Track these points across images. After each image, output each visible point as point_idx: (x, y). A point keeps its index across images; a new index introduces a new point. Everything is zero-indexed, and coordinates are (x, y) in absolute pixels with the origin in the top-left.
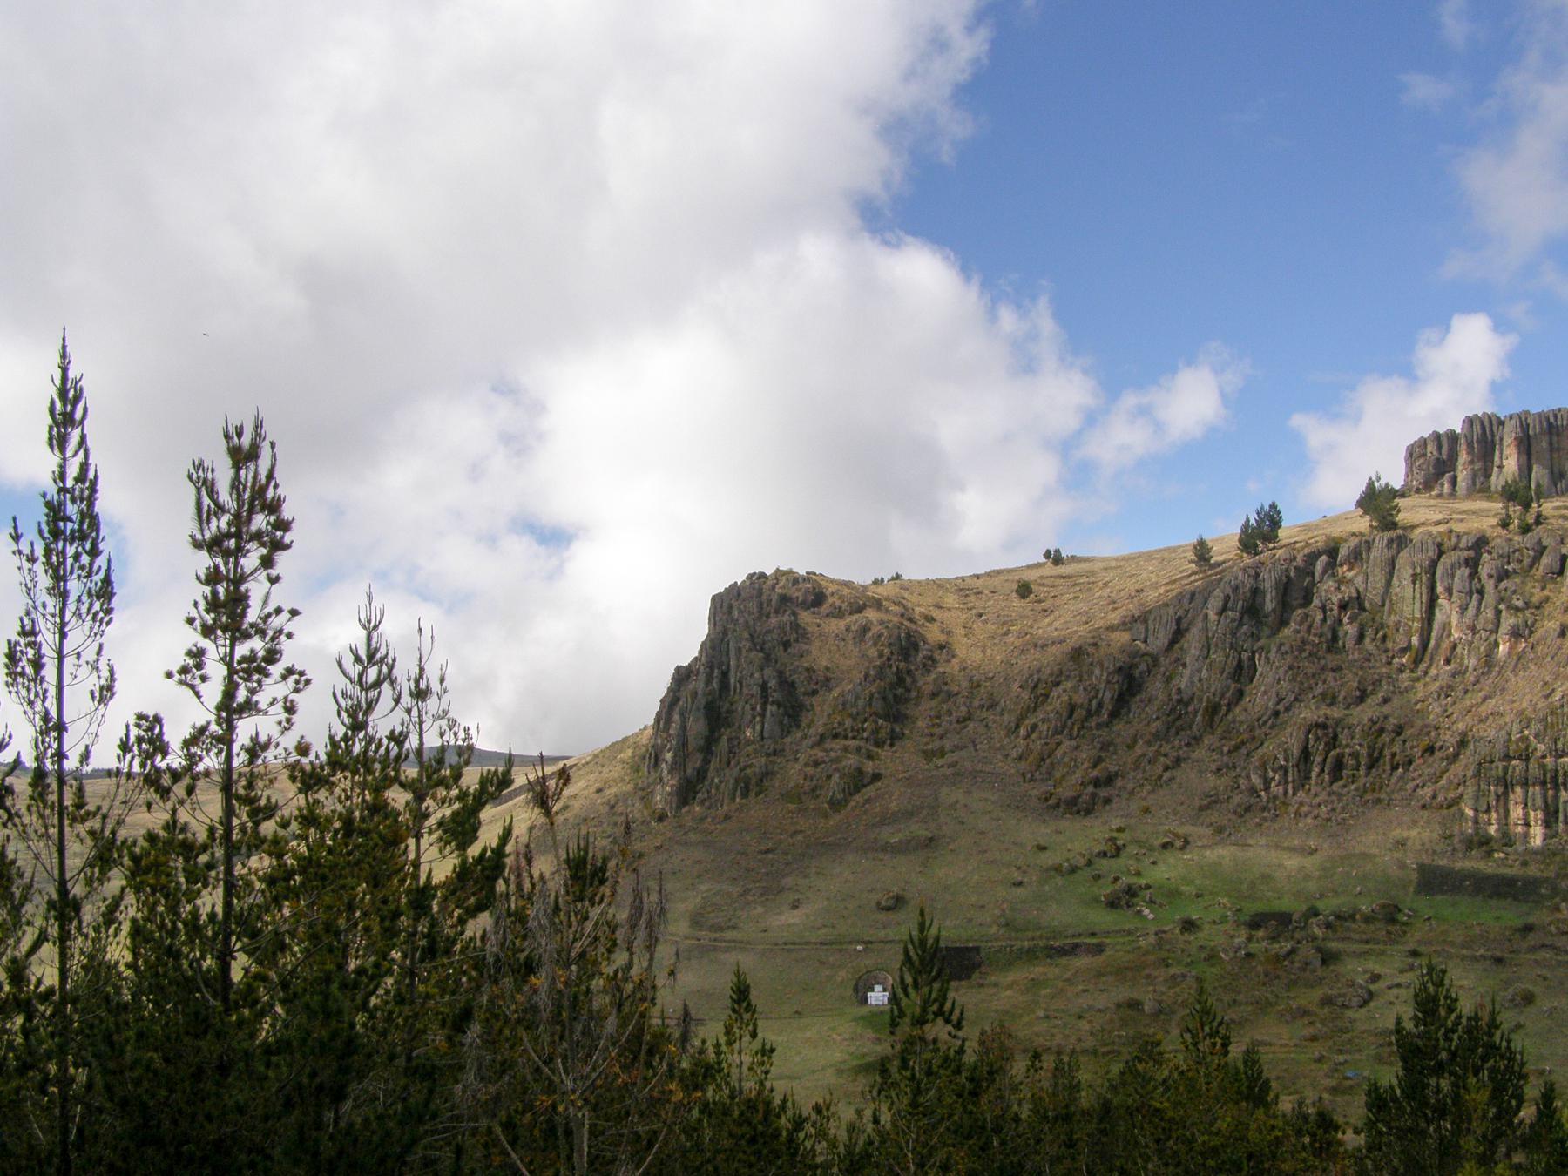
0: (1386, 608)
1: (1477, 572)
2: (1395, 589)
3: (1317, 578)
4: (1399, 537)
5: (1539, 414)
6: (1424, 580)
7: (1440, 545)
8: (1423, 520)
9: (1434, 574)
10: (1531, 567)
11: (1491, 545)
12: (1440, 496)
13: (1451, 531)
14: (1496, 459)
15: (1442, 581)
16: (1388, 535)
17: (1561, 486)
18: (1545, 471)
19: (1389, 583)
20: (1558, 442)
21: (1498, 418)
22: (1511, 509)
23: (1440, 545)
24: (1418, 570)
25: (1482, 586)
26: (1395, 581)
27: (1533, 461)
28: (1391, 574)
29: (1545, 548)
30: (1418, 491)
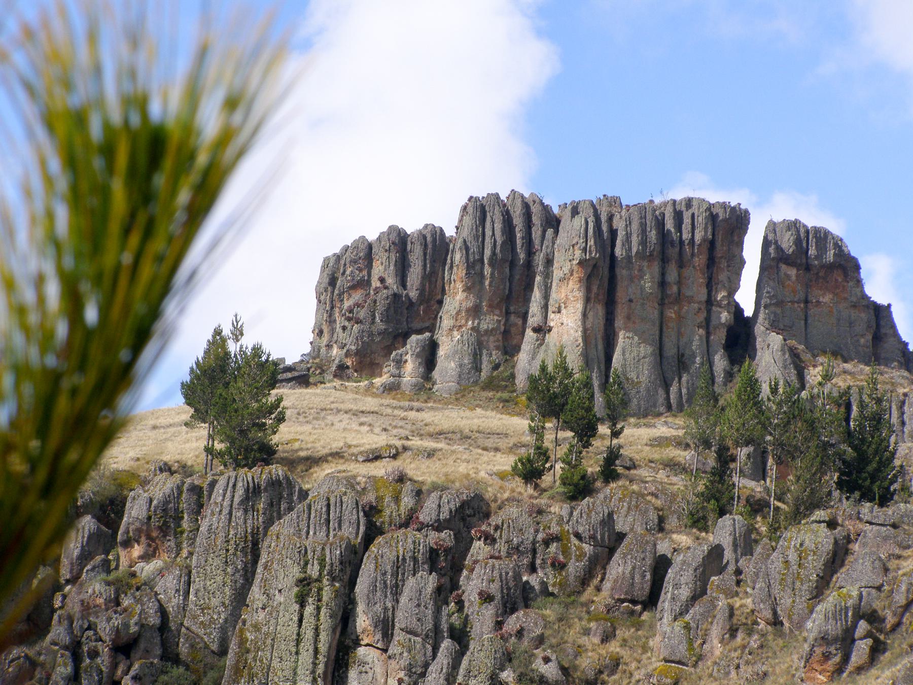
0: (230, 659)
1: (455, 586)
2: (254, 615)
3: (65, 573)
4: (275, 484)
5: (642, 209)
6: (327, 594)
7: (371, 511)
8: (336, 445)
9: (352, 583)
10: (584, 582)
11: (494, 520)
12: (392, 389)
13: (401, 479)
14: (534, 308)
15: (370, 603)
16: (247, 475)
17: (678, 389)
18: (646, 350)
19: (240, 598)
20: (679, 283)
21: (546, 209)
22: (549, 437)
23: (371, 511)
24: (314, 571)
25: (466, 621)
26: (256, 594)
27: (619, 322)
28: (248, 576)
29: (621, 537)
30: (341, 371)
